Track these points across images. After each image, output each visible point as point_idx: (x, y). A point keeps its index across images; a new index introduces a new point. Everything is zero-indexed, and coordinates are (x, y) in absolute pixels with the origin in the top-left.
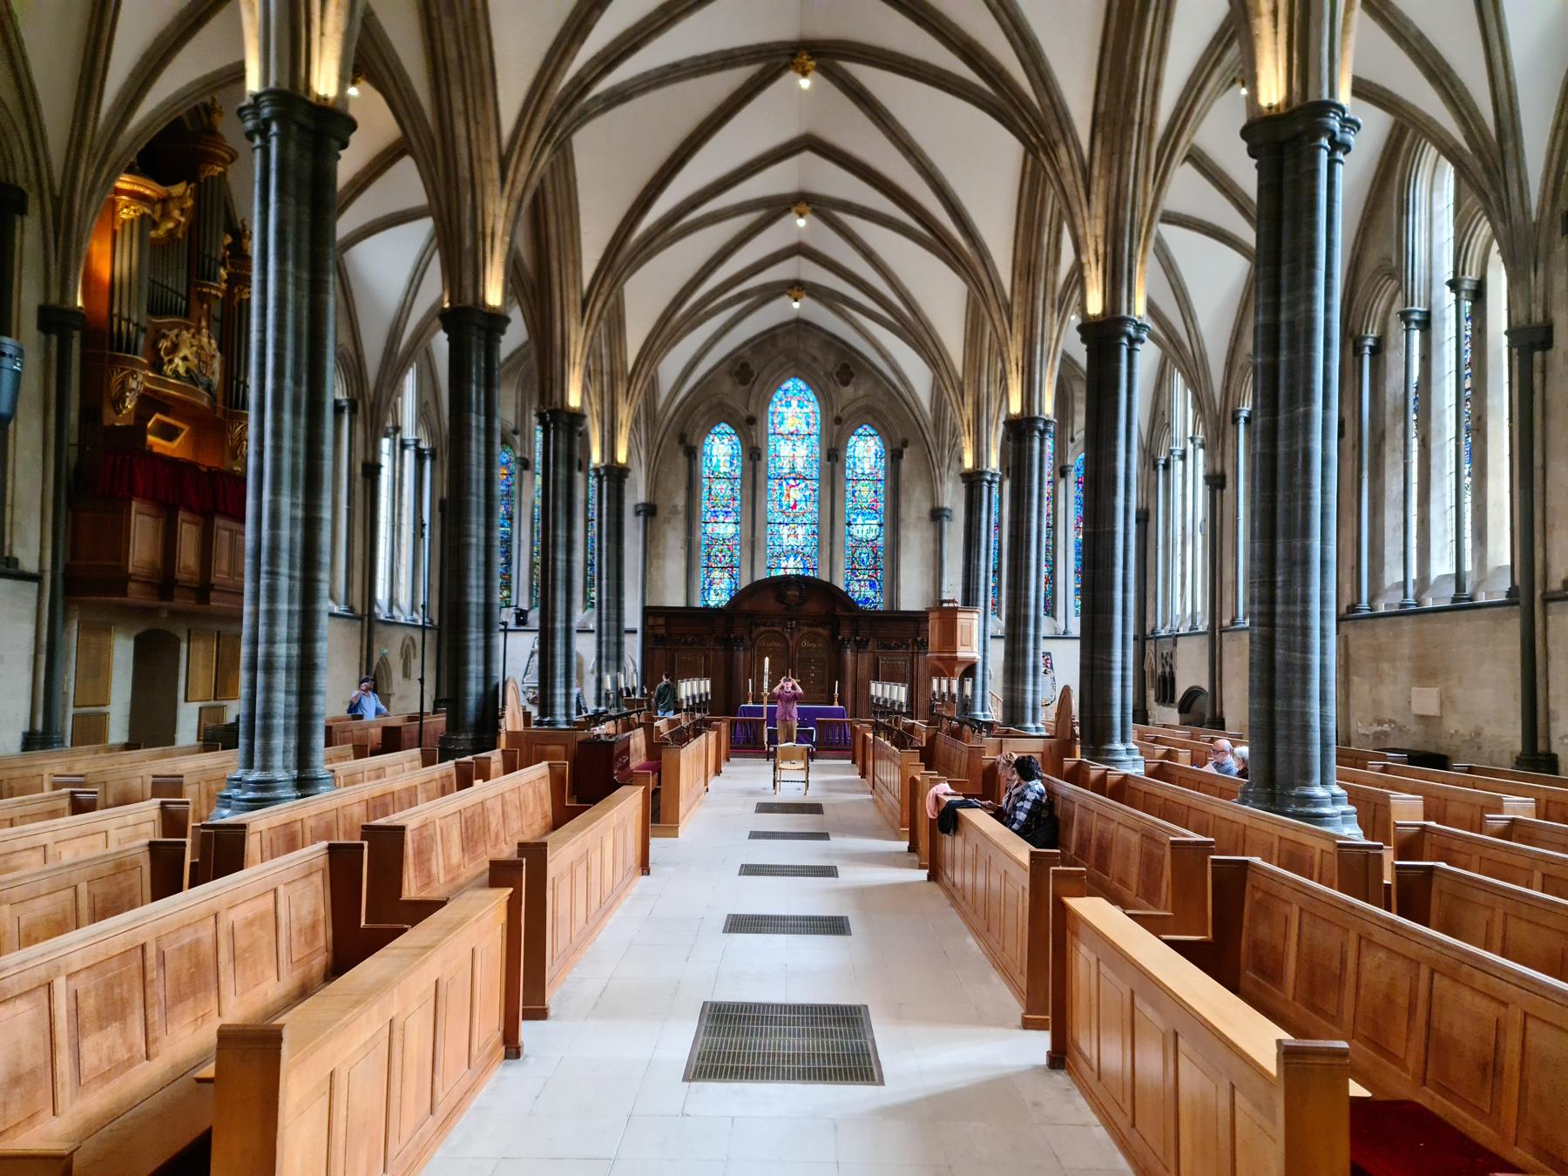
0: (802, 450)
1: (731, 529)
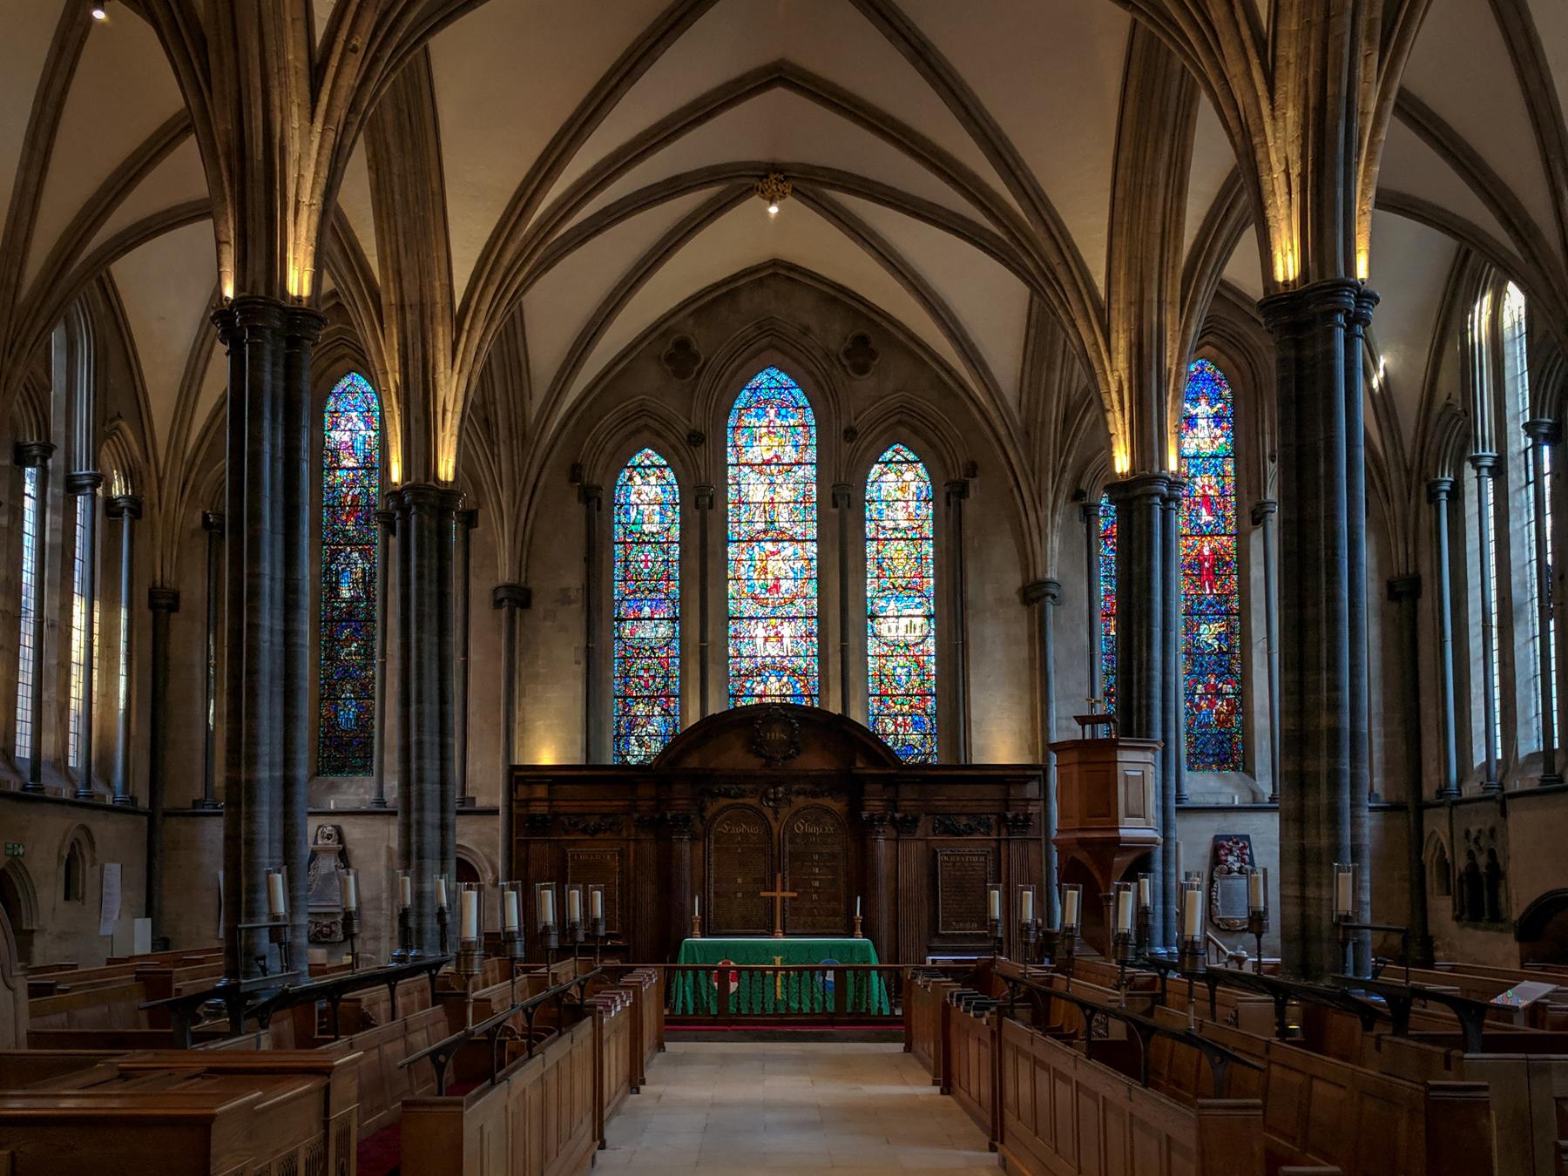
0: (786, 494)
1: (664, 630)
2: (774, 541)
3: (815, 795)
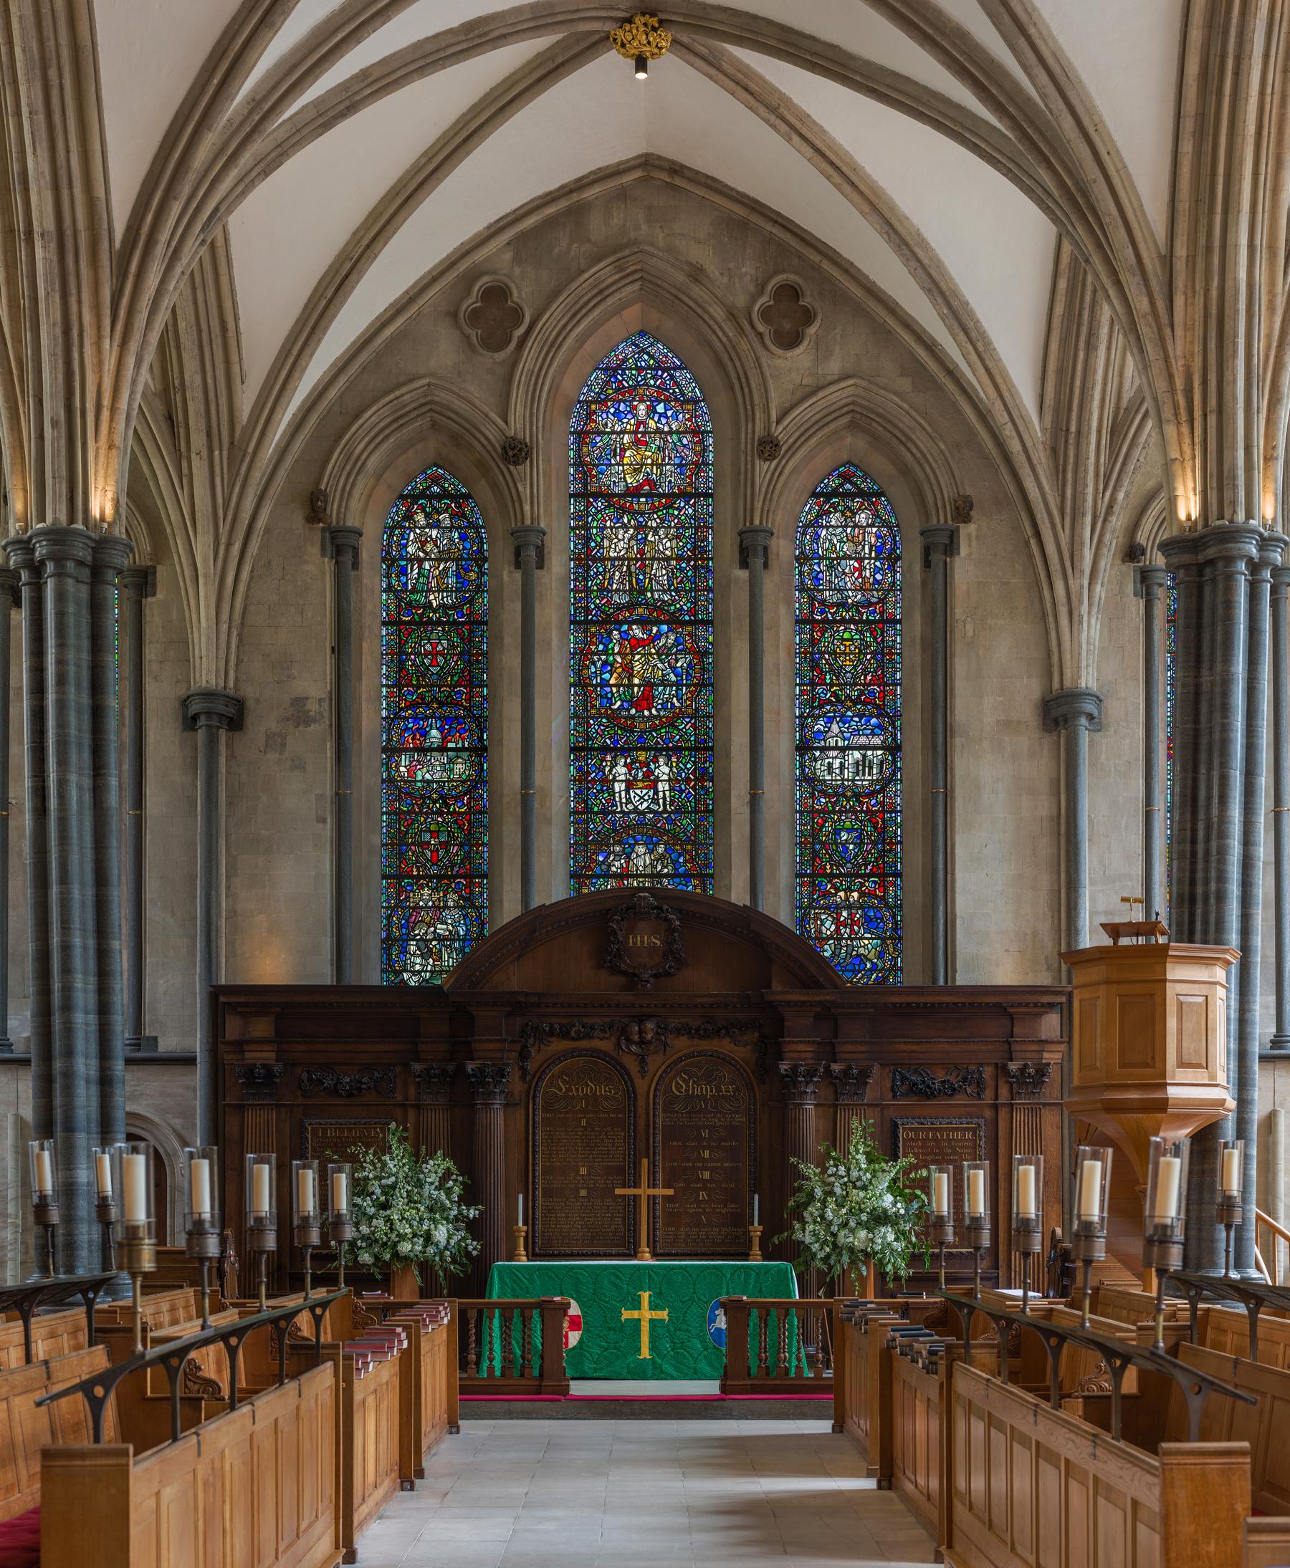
2: (644, 623)
3: (705, 1035)
